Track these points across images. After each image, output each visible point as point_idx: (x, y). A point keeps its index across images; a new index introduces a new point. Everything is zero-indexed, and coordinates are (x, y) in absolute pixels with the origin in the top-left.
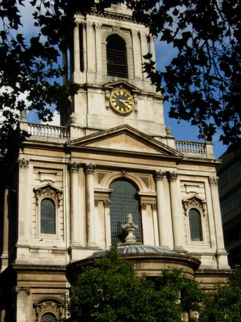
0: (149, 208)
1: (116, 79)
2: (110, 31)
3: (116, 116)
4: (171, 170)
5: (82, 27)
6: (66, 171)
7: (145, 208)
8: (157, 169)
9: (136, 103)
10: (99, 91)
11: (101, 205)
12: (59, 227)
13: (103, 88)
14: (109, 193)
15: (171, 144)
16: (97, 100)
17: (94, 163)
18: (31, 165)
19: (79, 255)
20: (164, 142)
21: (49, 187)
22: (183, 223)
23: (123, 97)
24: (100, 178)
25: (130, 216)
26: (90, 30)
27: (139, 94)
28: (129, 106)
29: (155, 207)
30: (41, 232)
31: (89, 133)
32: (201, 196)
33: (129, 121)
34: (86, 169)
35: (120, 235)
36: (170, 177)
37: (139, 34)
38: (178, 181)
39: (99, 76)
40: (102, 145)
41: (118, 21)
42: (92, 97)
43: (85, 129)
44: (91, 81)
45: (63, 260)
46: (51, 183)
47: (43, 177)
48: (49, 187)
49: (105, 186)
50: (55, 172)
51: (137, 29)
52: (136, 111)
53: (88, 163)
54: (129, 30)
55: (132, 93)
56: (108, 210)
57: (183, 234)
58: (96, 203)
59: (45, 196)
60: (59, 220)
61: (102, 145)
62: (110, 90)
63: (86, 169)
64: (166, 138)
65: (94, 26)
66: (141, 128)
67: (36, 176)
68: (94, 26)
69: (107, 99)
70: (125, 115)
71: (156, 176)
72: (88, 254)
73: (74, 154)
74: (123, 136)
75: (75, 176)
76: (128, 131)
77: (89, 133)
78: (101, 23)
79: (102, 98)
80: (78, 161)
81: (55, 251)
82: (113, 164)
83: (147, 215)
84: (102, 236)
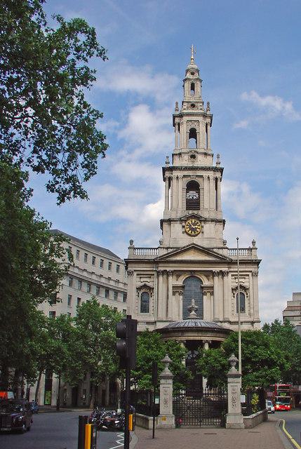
0: (209, 294)
1: (191, 212)
2: (189, 179)
3: (189, 237)
4: (223, 269)
5: (170, 179)
6: (156, 275)
7: (206, 295)
8: (214, 269)
9: (202, 227)
10: (179, 222)
11: (177, 294)
12: (151, 308)
13: (181, 220)
14: (183, 287)
15: (225, 252)
16: (177, 227)
17: (172, 269)
18: (135, 273)
19: (160, 326)
20: (220, 252)
21: (145, 286)
22: (231, 302)
23: (194, 224)
24: (178, 276)
25: (193, 300)
26: (174, 182)
27: (206, 221)
28: (198, 230)
29: (212, 294)
30: (142, 312)
31: (170, 250)
32: (246, 284)
33: (197, 241)
34: (165, 273)
35: (187, 312)
36: (222, 274)
37: (209, 178)
38: (230, 274)
39: (179, 212)
40: (178, 258)
41: (194, 172)
42: (174, 226)
43: (167, 248)
44: (173, 216)
45: (151, 328)
46: (147, 283)
47: (142, 280)
48: (145, 286)
49: (180, 283)
50: (150, 276)
51: (207, 175)
52: (203, 232)
53: (168, 269)
54: (202, 176)
55: (201, 221)
56: (181, 297)
57: (230, 309)
58: (174, 294)
59: (144, 290)
60: (151, 304)
61: (178, 258)
62: (186, 221)
63: (165, 273)
64: (222, 248)
65: (177, 177)
66: (205, 244)
67: (138, 279)
68: (177, 177)
69: (183, 227)
70: (196, 235)
71: (213, 274)
72: (167, 324)
73: (160, 265)
74: (192, 252)
75: (161, 278)
76: (194, 248)
77: (170, 250)
78: (182, 175)
79: (181, 226)
80: (162, 269)
81: (148, 323)
82: (185, 269)
83: (206, 299)
84: (177, 313)
